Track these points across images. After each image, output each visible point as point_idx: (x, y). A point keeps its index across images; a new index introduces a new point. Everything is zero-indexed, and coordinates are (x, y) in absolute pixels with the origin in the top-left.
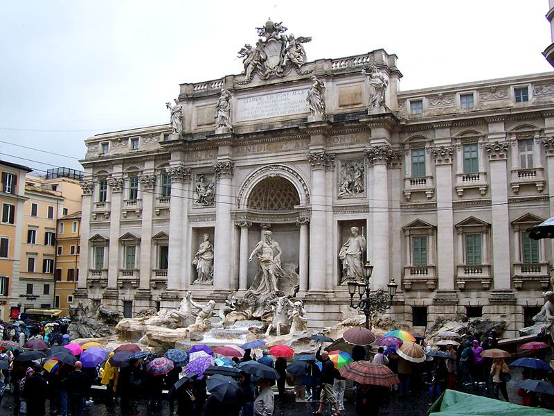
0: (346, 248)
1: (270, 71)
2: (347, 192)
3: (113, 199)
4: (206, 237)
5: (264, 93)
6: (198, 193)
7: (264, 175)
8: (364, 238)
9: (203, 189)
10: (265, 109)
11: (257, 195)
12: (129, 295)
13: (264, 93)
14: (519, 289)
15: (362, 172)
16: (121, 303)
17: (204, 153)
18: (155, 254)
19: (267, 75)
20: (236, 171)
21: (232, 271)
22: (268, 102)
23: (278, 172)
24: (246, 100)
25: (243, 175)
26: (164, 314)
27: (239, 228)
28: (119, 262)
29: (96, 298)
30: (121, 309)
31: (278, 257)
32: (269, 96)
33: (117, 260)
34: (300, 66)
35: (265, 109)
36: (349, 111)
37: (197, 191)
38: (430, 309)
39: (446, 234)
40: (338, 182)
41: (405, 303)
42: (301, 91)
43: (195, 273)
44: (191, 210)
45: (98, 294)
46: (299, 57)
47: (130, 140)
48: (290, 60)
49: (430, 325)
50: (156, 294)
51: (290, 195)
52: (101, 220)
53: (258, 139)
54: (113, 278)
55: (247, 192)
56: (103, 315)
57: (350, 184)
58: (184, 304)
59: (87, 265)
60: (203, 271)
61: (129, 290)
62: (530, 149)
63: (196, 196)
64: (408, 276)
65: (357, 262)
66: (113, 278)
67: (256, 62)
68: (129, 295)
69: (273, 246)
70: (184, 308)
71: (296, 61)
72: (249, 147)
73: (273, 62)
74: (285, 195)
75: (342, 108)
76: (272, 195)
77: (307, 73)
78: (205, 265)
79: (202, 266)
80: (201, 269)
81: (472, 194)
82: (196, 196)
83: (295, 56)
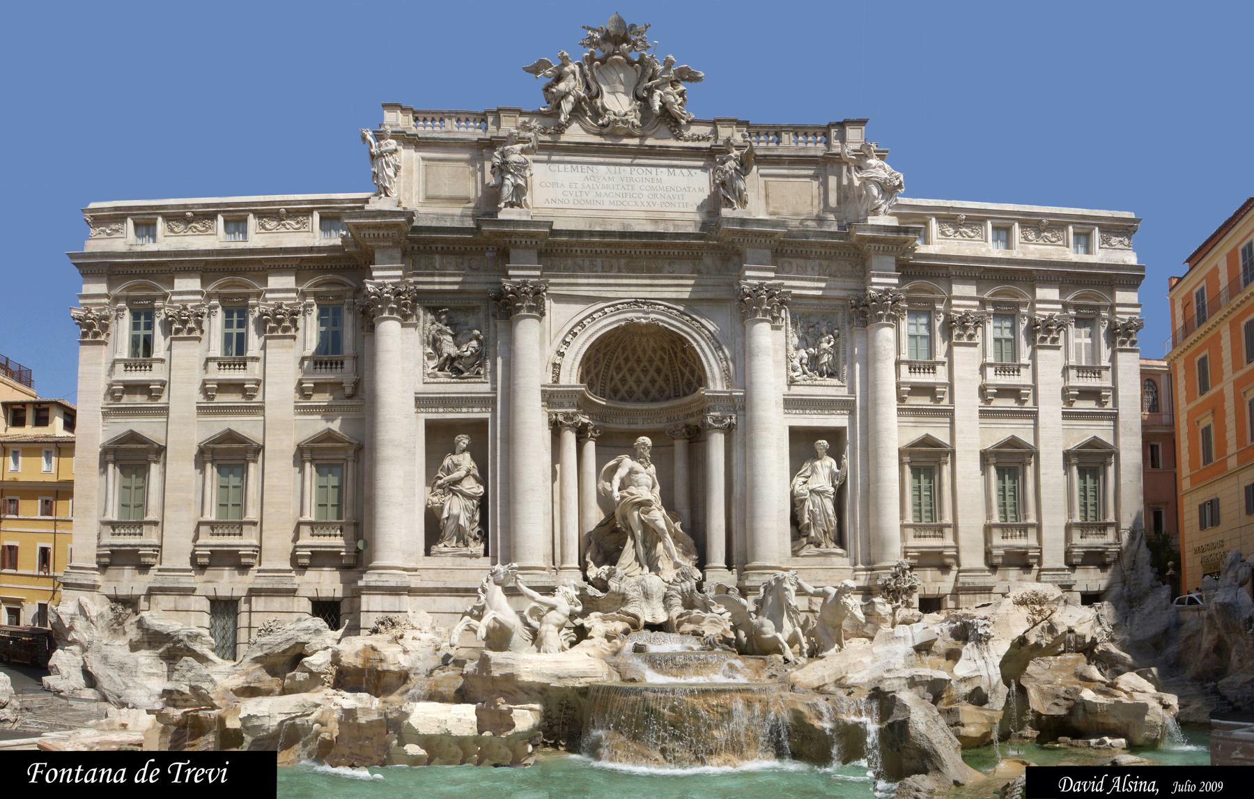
11: (592, 363)
12: (227, 583)
25: (559, 315)
29: (123, 591)
32: (612, 168)
34: (683, 122)
42: (684, 171)
43: (435, 529)
44: (421, 387)
45: (130, 582)
48: (664, 107)
54: (177, 542)
56: (152, 639)
60: (461, 522)
66: (177, 542)
68: (227, 583)
71: (676, 109)
77: (698, 140)
78: (466, 508)
79: (458, 509)
80: (458, 517)
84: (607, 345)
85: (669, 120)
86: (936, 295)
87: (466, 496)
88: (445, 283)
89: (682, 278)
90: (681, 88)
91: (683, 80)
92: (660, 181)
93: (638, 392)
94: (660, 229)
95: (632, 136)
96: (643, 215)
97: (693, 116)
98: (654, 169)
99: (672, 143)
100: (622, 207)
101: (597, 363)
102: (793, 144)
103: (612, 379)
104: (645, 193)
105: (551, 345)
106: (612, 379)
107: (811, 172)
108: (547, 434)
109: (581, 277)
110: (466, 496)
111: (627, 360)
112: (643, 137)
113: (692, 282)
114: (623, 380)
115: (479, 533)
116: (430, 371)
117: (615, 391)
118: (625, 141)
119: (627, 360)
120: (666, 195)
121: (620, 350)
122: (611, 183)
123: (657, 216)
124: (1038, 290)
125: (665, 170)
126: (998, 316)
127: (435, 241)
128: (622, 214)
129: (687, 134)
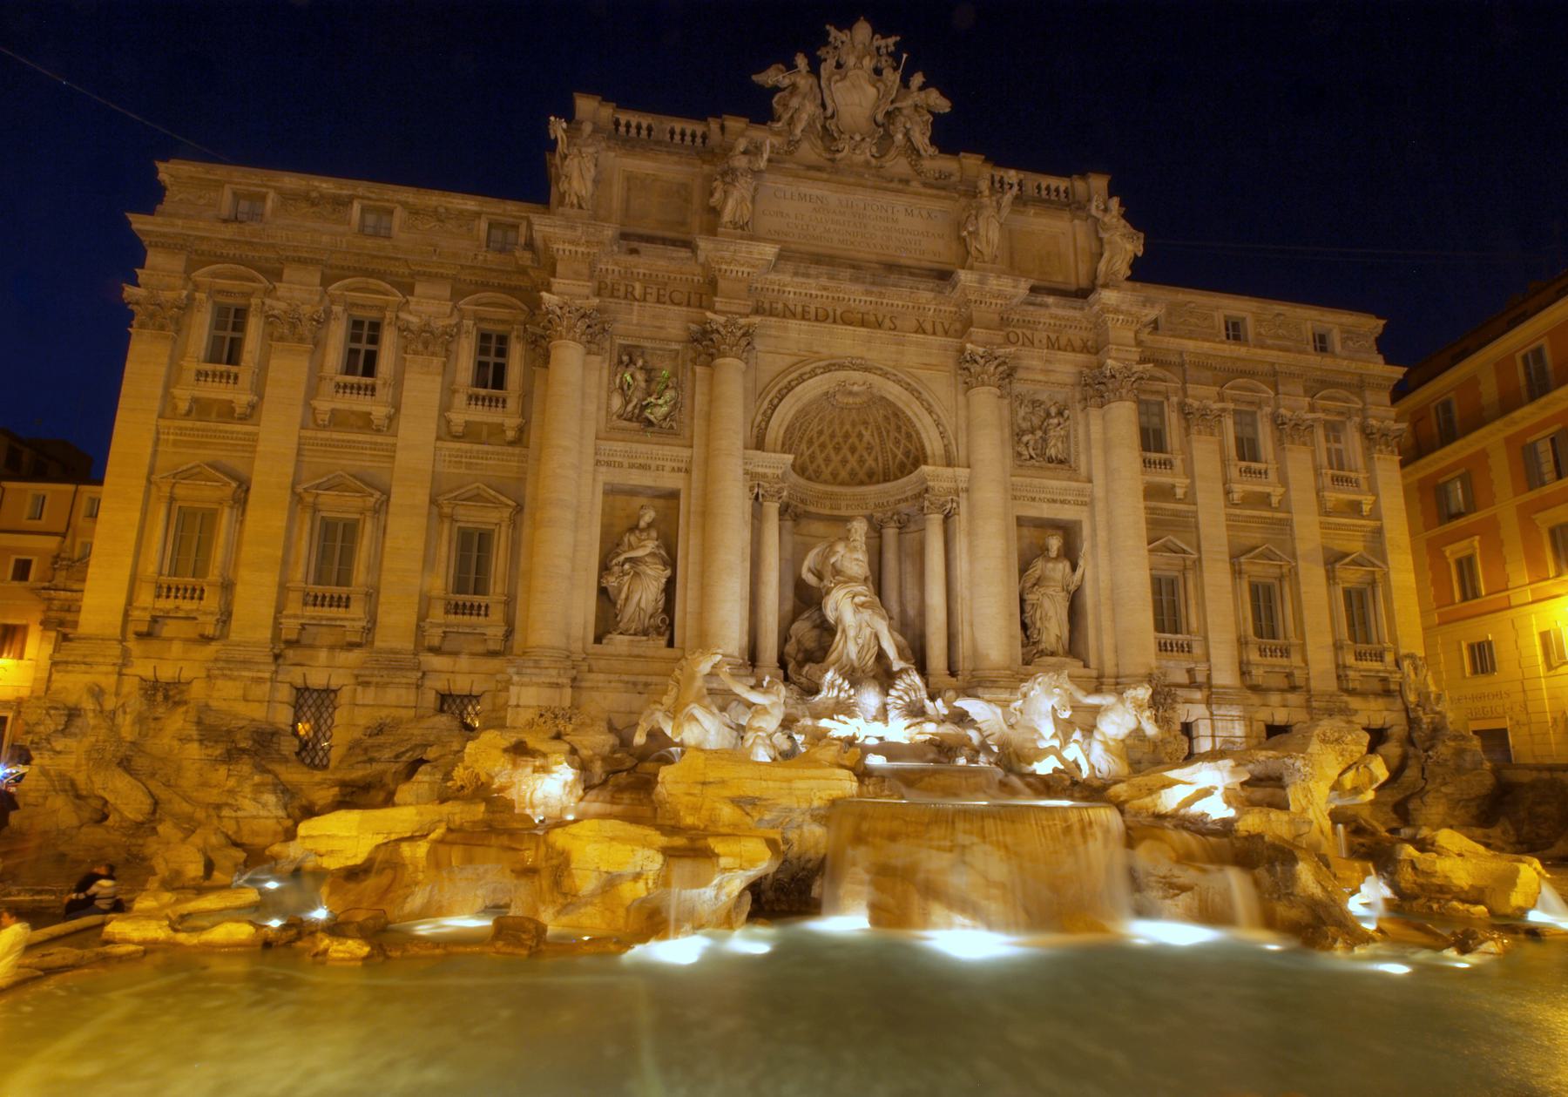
3: (274, 363)
9: (643, 384)
14: (1352, 692)
16: (285, 693)
18: (444, 549)
28: (285, 562)
30: (284, 716)
33: (280, 553)
37: (623, 389)
47: (356, 206)
51: (853, 450)
53: (825, 289)
59: (129, 561)
61: (323, 655)
62: (1337, 440)
74: (837, 449)
76: (810, 442)
82: (617, 402)
115: (663, 621)
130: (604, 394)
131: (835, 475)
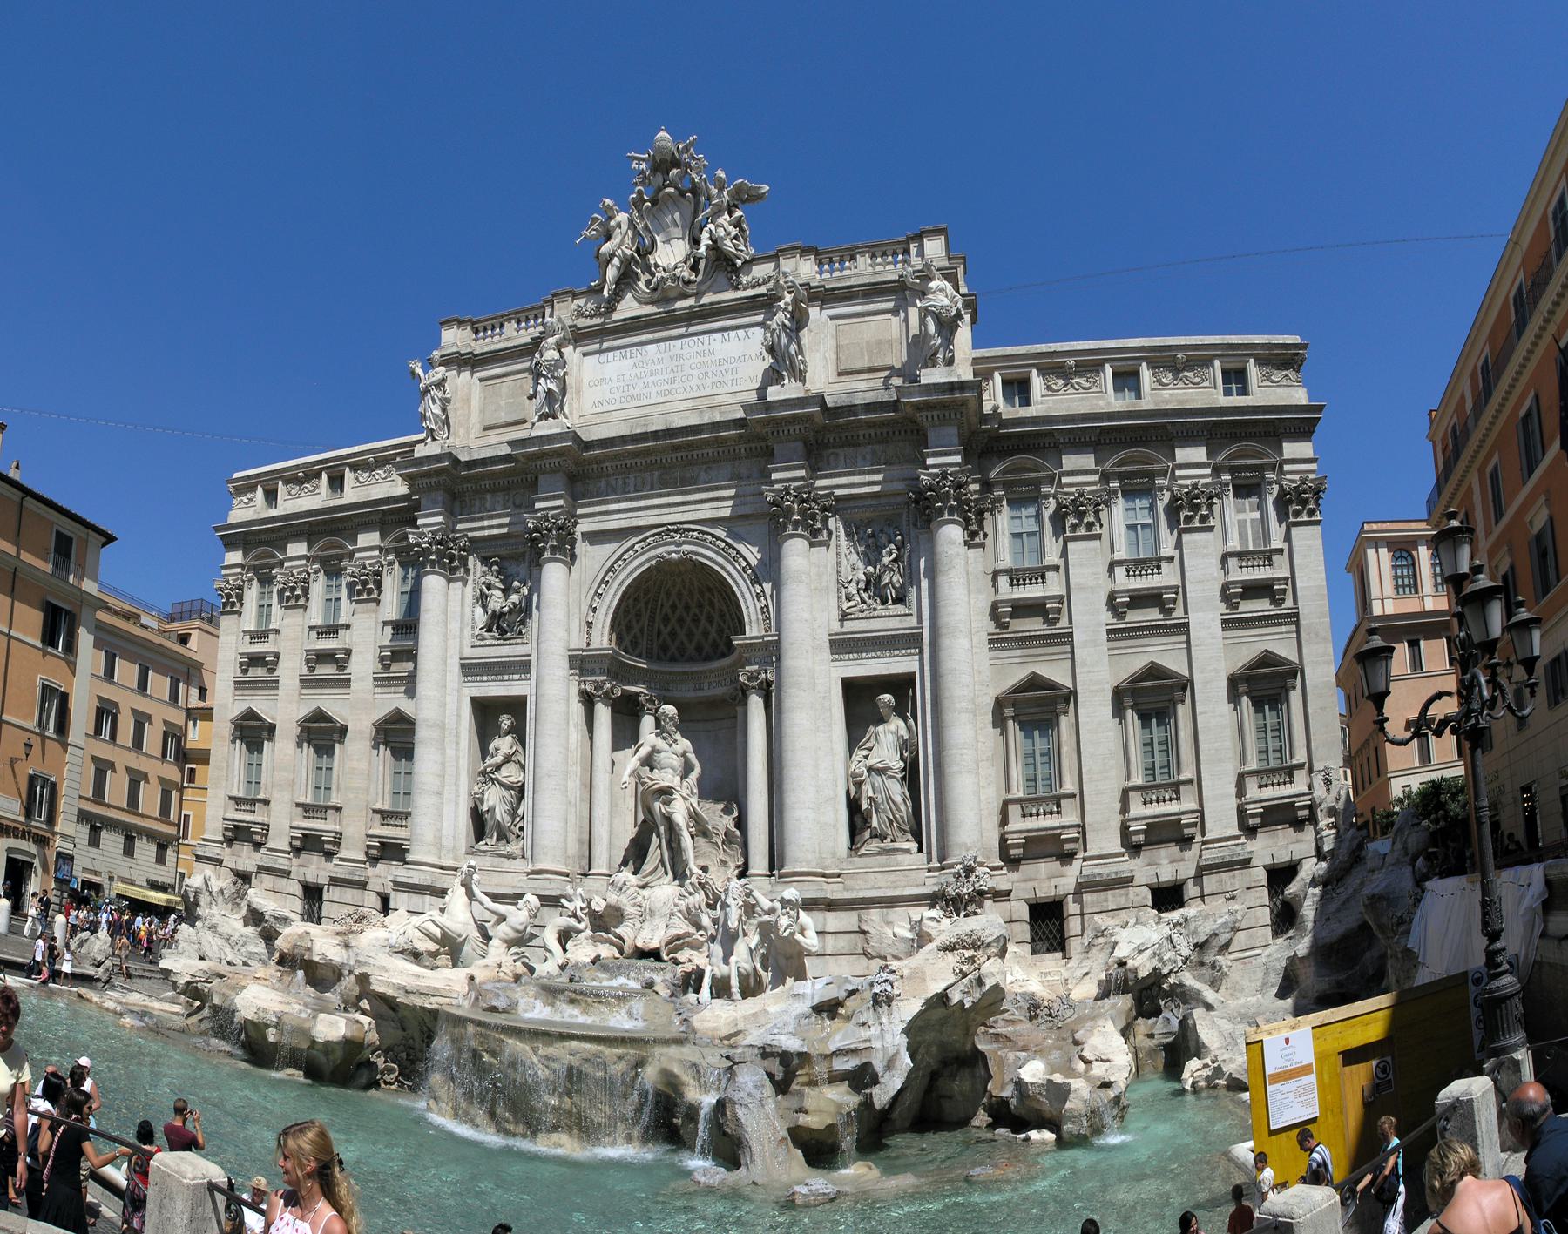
0: (864, 753)
1: (666, 275)
2: (863, 601)
4: (506, 722)
5: (650, 336)
6: (484, 607)
7: (652, 553)
8: (911, 721)
9: (498, 593)
10: (651, 379)
13: (650, 336)
15: (898, 549)
17: (500, 497)
19: (654, 289)
20: (581, 548)
21: (572, 819)
22: (660, 361)
23: (685, 547)
24: (604, 357)
25: (592, 558)
26: (405, 925)
27: (588, 701)
31: (694, 776)
34: (739, 262)
35: (651, 379)
36: (862, 385)
38: (1072, 907)
39: (1095, 709)
40: (838, 572)
41: (1013, 896)
42: (741, 332)
44: (468, 652)
46: (736, 238)
48: (715, 245)
49: (1074, 946)
50: (384, 874)
52: (258, 673)
55: (612, 596)
57: (868, 582)
58: (457, 896)
63: (481, 617)
64: (1016, 823)
65: (897, 791)
67: (629, 252)
69: (679, 748)
70: (458, 915)
71: (728, 245)
72: (612, 480)
73: (670, 254)
75: (844, 378)
81: (1146, 608)
83: (728, 234)
84: (647, 592)
85: (722, 265)
86: (1044, 474)
87: (502, 785)
88: (482, 528)
89: (717, 488)
90: (739, 213)
91: (743, 202)
92: (712, 352)
93: (691, 648)
94: (706, 419)
95: (685, 296)
96: (688, 404)
97: (752, 251)
98: (705, 338)
99: (731, 295)
100: (670, 398)
101: (639, 615)
102: (870, 269)
103: (659, 633)
104: (695, 373)
105: (573, 604)
106: (659, 633)
107: (891, 305)
108: (577, 709)
109: (612, 502)
110: (502, 785)
111: (674, 607)
112: (698, 295)
113: (732, 492)
114: (673, 634)
116: (477, 632)
117: (664, 648)
118: (679, 305)
119: (674, 607)
120: (707, 374)
121: (663, 595)
122: (659, 366)
123: (706, 402)
124: (1178, 451)
125: (719, 335)
126: (1129, 494)
127: (483, 476)
128: (669, 407)
129: (745, 279)
130: (468, 610)
131: (682, 650)
